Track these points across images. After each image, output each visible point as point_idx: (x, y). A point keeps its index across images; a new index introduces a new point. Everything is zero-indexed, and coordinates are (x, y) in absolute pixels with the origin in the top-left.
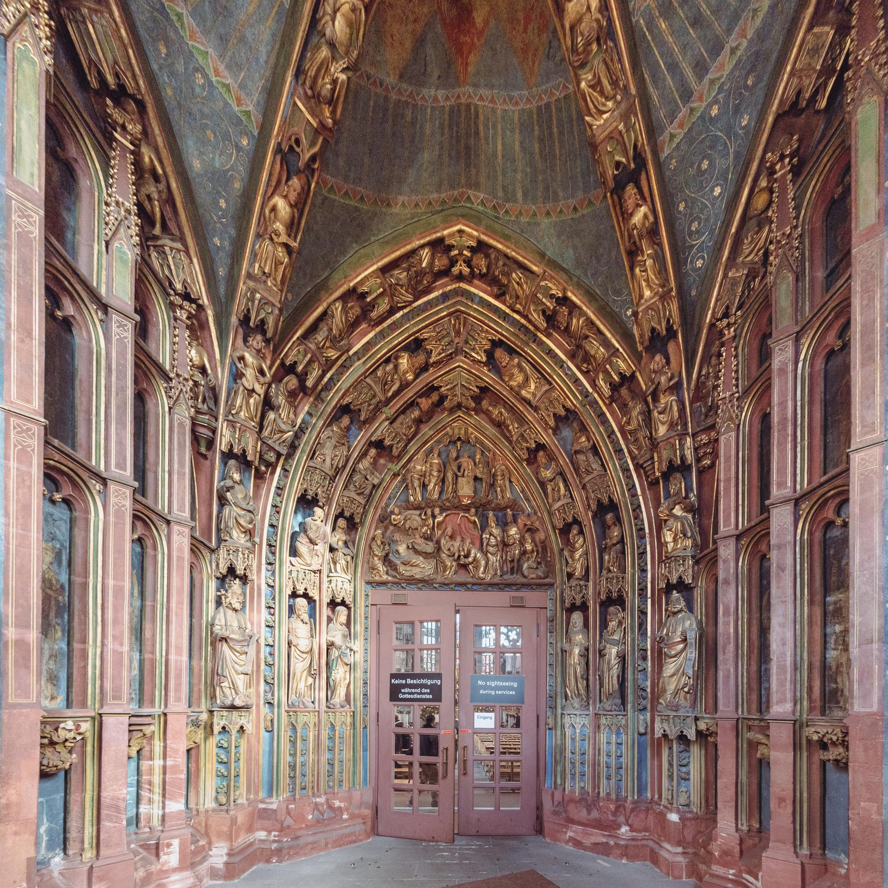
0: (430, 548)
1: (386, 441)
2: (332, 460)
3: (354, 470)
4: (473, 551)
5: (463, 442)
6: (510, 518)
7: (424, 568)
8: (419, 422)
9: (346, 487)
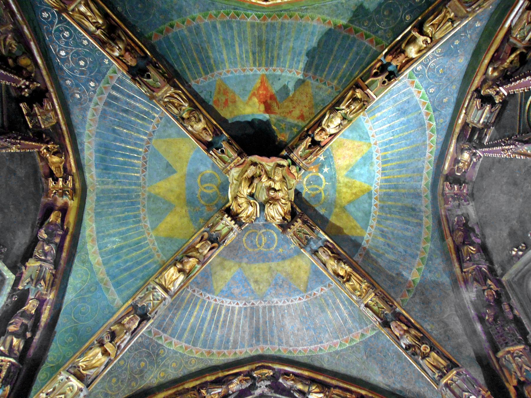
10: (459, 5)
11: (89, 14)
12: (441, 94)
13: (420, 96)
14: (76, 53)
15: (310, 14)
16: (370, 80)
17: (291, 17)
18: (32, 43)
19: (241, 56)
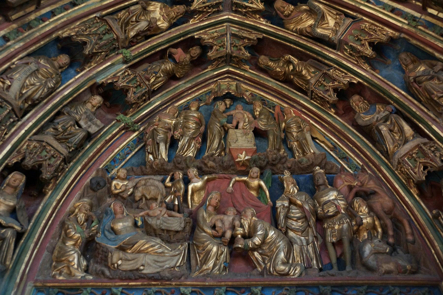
1: (119, 82)
2: (23, 87)
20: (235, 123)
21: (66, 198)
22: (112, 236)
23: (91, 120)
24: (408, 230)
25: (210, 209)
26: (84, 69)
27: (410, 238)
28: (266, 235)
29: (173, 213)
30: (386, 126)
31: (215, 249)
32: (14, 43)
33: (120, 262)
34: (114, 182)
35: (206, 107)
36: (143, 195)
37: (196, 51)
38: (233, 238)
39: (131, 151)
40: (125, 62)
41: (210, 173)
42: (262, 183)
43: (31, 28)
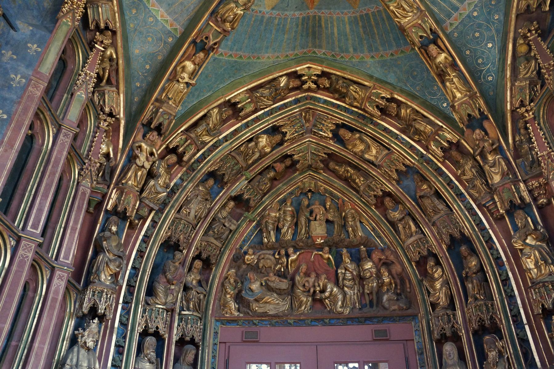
0: (284, 284)
3: (214, 219)
4: (329, 286)
5: (313, 193)
6: (364, 254)
7: (275, 304)
8: (274, 179)
9: (206, 233)
10: (169, 111)
11: (455, 90)
12: (141, 17)
13: (160, 12)
14: (479, 44)
15: (271, 60)
16: (219, 39)
17: (287, 56)
18: (509, 62)
19: (333, 26)
20: (314, 216)
21: (223, 269)
22: (251, 293)
23: (231, 221)
24: (408, 286)
25: (301, 274)
26: (224, 188)
27: (408, 290)
28: (332, 291)
29: (282, 280)
30: (401, 224)
31: (305, 299)
32: (187, 184)
33: (257, 309)
34: (247, 257)
35: (296, 198)
36: (264, 266)
37: (288, 162)
38: (315, 292)
39: (253, 234)
40: (246, 179)
41: (301, 249)
42: (330, 257)
43: (194, 170)
